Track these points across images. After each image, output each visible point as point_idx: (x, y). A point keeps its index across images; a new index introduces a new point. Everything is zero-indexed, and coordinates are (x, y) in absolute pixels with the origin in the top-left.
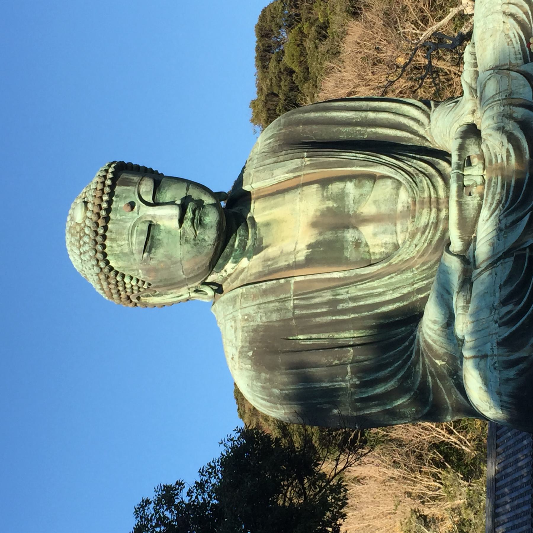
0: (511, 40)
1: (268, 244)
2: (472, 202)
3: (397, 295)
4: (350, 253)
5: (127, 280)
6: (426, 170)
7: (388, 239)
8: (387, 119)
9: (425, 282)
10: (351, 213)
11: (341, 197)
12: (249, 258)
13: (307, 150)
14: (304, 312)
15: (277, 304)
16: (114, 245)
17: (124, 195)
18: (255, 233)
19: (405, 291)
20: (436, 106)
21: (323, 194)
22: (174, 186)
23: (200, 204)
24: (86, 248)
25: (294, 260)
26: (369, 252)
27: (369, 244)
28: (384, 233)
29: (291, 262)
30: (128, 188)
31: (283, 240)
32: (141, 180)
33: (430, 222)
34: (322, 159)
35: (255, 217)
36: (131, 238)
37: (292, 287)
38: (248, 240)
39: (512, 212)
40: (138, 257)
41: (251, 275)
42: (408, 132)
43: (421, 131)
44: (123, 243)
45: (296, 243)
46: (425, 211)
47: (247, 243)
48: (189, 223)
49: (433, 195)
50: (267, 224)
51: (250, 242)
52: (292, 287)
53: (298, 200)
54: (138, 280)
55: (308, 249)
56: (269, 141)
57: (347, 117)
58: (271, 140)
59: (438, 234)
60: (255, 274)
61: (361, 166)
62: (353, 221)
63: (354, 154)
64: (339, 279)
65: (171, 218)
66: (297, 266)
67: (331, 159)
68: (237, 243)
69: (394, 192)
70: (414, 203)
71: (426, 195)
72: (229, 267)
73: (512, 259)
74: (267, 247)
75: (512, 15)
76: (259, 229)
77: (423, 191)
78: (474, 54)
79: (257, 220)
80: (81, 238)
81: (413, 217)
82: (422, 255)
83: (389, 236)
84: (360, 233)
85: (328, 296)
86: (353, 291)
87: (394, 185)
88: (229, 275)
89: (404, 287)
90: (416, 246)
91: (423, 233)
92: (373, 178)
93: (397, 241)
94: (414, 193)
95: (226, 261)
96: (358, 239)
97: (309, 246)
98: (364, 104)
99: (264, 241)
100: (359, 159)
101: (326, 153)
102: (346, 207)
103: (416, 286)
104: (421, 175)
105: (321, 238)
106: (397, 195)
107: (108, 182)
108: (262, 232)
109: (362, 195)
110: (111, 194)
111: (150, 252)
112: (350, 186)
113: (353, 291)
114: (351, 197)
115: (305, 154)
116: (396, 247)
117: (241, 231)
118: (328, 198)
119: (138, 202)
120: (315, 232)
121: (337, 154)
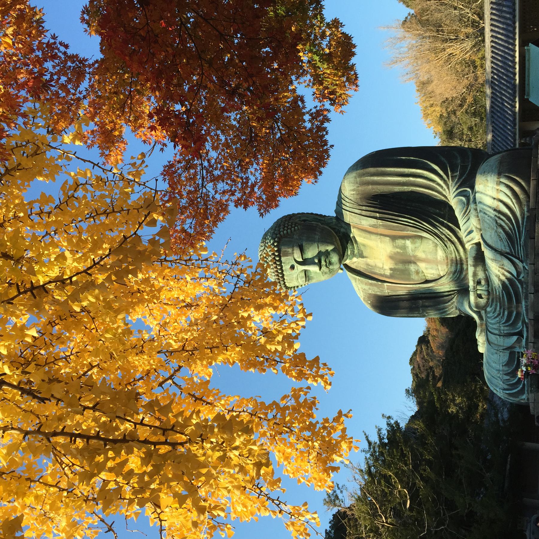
4: (414, 277)
7: (434, 272)
11: (404, 248)
13: (377, 210)
22: (311, 248)
23: (327, 254)
28: (431, 268)
29: (383, 273)
39: (507, 326)
43: (444, 193)
49: (458, 258)
50: (364, 245)
51: (356, 251)
62: (413, 259)
69: (434, 248)
73: (508, 352)
75: (501, 226)
84: (418, 266)
97: (391, 269)
105: (397, 267)
106: (436, 250)
108: (362, 248)
112: (408, 243)
114: (410, 248)
117: (349, 246)
119: (296, 265)
120: (393, 262)
121: (396, 218)
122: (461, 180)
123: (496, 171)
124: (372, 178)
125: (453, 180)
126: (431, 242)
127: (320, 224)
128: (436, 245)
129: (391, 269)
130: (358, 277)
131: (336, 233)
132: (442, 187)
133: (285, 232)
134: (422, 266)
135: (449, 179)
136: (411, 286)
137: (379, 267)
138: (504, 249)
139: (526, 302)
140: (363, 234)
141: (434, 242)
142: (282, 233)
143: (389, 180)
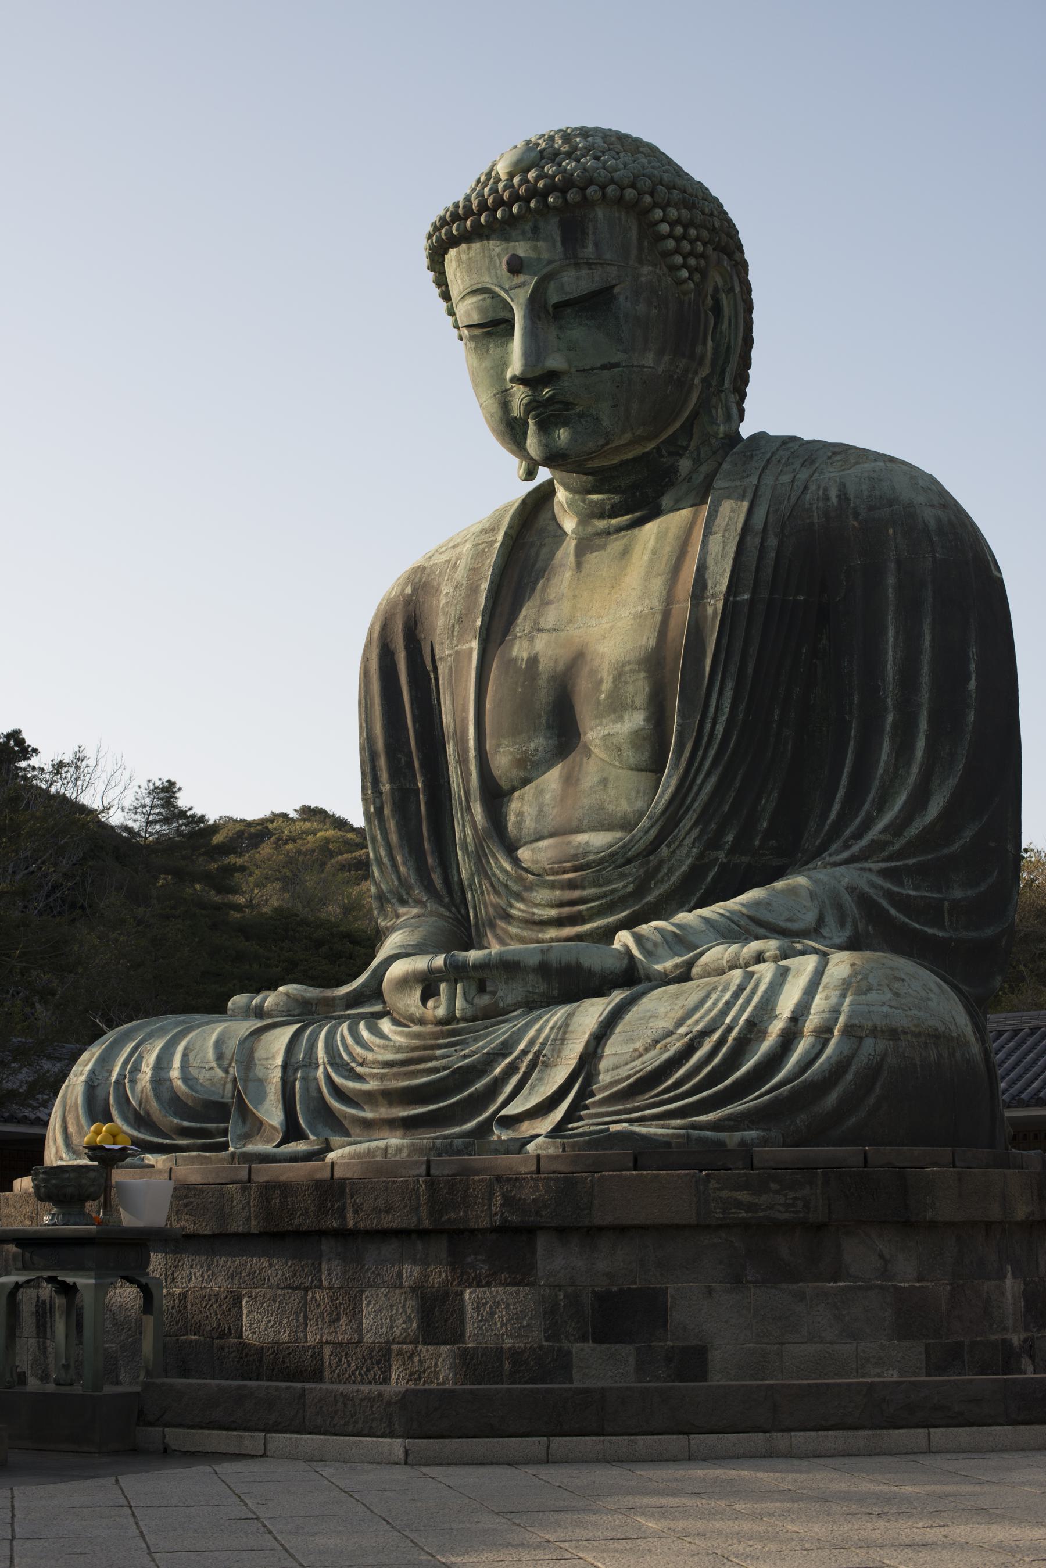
0: (641, 1056)
1: (586, 567)
6: (662, 881)
8: (878, 761)
11: (616, 706)
18: (619, 529)
21: (629, 663)
25: (519, 634)
26: (514, 789)
30: (559, 244)
32: (589, 265)
33: (535, 910)
36: (468, 294)
38: (610, 517)
41: (542, 545)
42: (841, 815)
43: (834, 848)
44: (459, 281)
47: (601, 516)
48: (525, 401)
50: (626, 552)
53: (639, 609)
55: (529, 659)
58: (834, 500)
60: (537, 555)
63: (727, 710)
68: (595, 497)
73: (228, 1098)
74: (579, 565)
75: (690, 1049)
76: (625, 536)
77: (596, 884)
79: (649, 526)
83: (533, 825)
92: (655, 766)
93: (524, 845)
94: (599, 864)
97: (533, 661)
98: (925, 696)
99: (594, 554)
100: (708, 726)
101: (738, 646)
102: (597, 721)
104: (641, 871)
105: (542, 681)
106: (610, 828)
108: (616, 544)
109: (620, 750)
112: (635, 720)
115: (746, 597)
118: (619, 677)
121: (733, 669)
122: (884, 903)
123: (901, 1020)
124: (892, 565)
125: (882, 873)
126: (640, 804)
127: (705, 372)
128: (626, 825)
129: (533, 661)
130: (500, 537)
131: (672, 440)
132: (858, 835)
133: (665, 228)
135: (889, 858)
136: (472, 743)
137: (539, 614)
138: (603, 1065)
139: (399, 1150)
140: (668, 548)
141: (641, 815)
142: (658, 214)
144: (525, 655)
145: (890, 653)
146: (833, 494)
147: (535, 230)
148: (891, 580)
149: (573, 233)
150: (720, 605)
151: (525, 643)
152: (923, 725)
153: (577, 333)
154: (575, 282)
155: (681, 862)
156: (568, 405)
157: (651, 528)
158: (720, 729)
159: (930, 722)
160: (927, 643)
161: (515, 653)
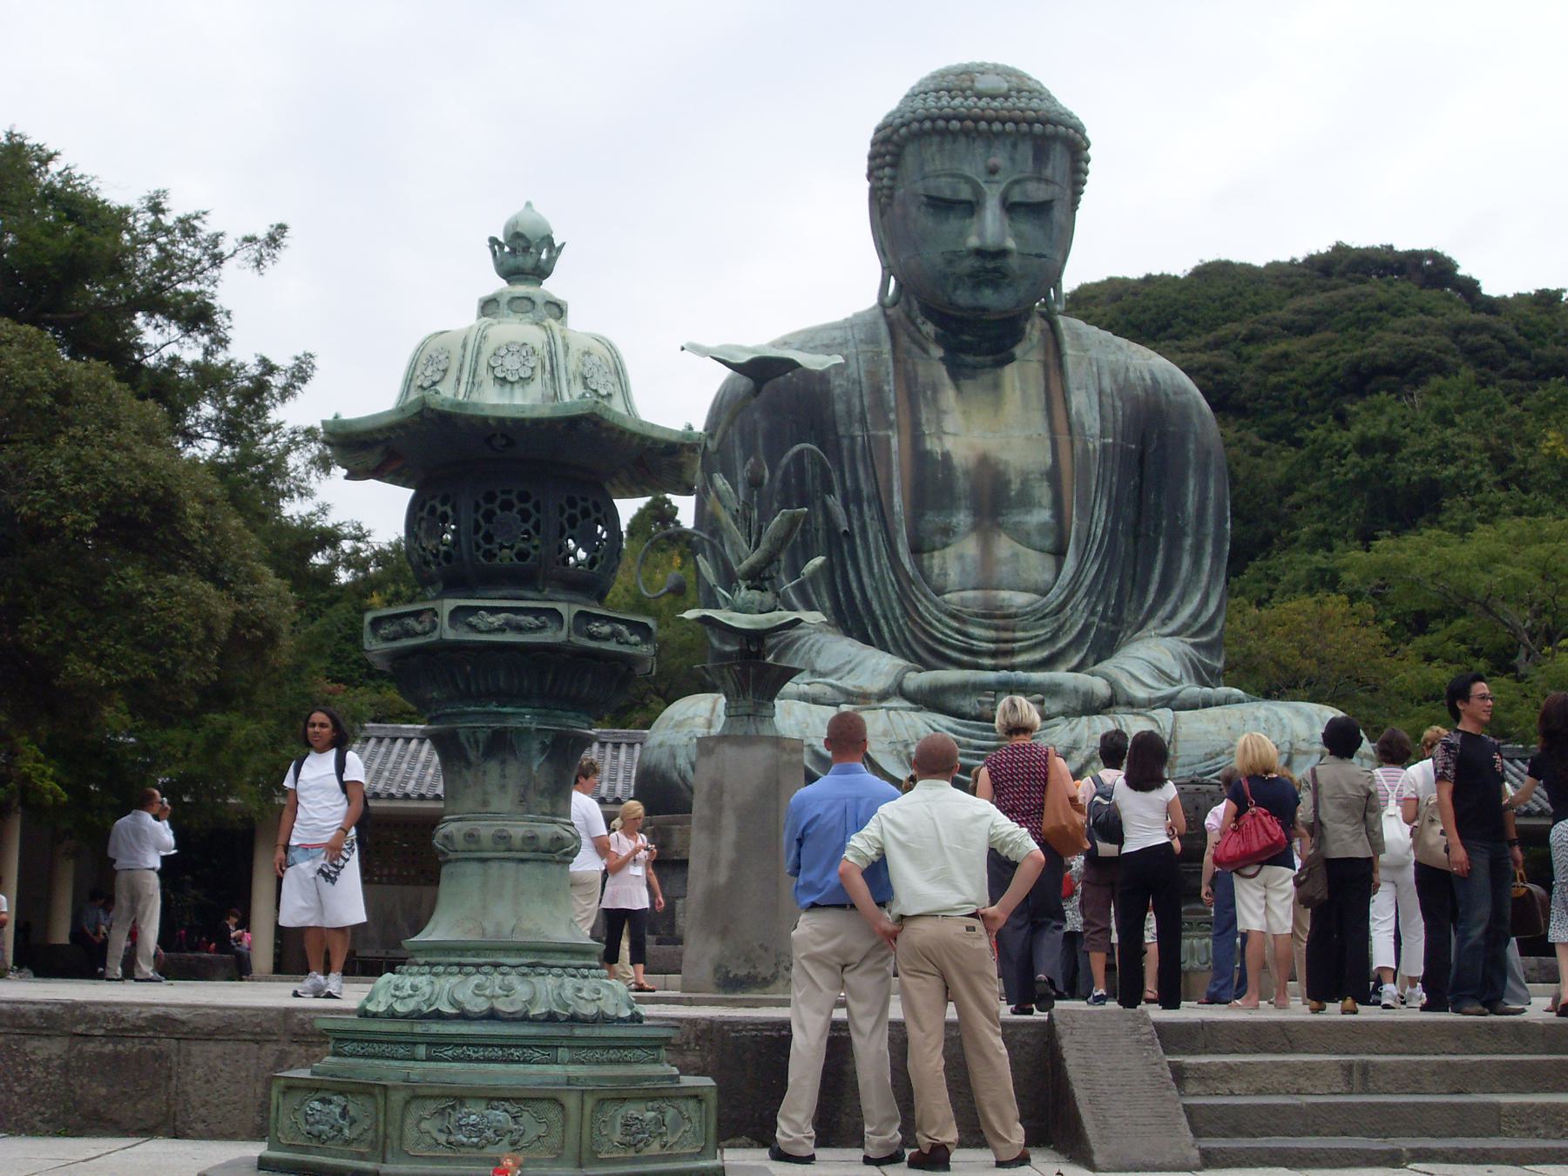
2: (969, 704)
3: (870, 593)
4: (932, 519)
5: (887, 171)
7: (953, 576)
8: (1179, 568)
9: (887, 636)
10: (1000, 519)
11: (1026, 501)
12: (942, 359)
13: (1119, 441)
14: (845, 453)
15: (858, 410)
16: (934, 148)
17: (1018, 157)
18: (984, 367)
19: (875, 605)
20: (1194, 645)
24: (931, 102)
26: (934, 549)
27: (948, 550)
28: (963, 571)
31: (964, 412)
32: (1047, 181)
34: (1095, 469)
35: (1014, 365)
37: (881, 433)
40: (919, 187)
41: (914, 364)
42: (1154, 601)
45: (955, 435)
46: (992, 634)
48: (977, 264)
50: (996, 387)
51: (969, 359)
52: (881, 433)
54: (891, 188)
56: (1147, 377)
57: (1184, 505)
58: (1149, 382)
59: (954, 654)
61: (1078, 532)
64: (891, 507)
65: (981, 235)
66: (917, 437)
67: (1094, 482)
70: (1009, 616)
71: (1020, 634)
72: (929, 328)
74: (958, 387)
77: (1024, 629)
78: (1227, 701)
80: (949, 91)
81: (984, 616)
82: (925, 631)
84: (966, 535)
85: (866, 489)
86: (873, 528)
87: (1042, 586)
88: (919, 330)
89: (881, 604)
90: (939, 621)
91: (958, 631)
95: (936, 324)
96: (955, 533)
97: (946, 456)
98: (1210, 528)
103: (882, 622)
105: (959, 473)
106: (1026, 590)
107: (1037, 127)
108: (986, 378)
109: (1028, 534)
110: (1016, 139)
111: (929, 205)
112: (1043, 515)
113: (873, 528)
116: (940, 591)
118: (1025, 482)
119: (1003, 180)
134: (969, 547)
135: (1193, 635)
138: (1180, 761)
143: (1183, 480)
144: (939, 450)
145: (1190, 496)
146: (1147, 377)
147: (1014, 146)
148: (1192, 446)
149: (1041, 156)
150: (1097, 444)
151: (936, 441)
152: (1209, 549)
153: (1027, 227)
154: (1036, 192)
155: (1076, 622)
156: (1005, 276)
157: (1010, 373)
158: (1099, 531)
159: (1214, 546)
160: (1212, 494)
161: (928, 446)
